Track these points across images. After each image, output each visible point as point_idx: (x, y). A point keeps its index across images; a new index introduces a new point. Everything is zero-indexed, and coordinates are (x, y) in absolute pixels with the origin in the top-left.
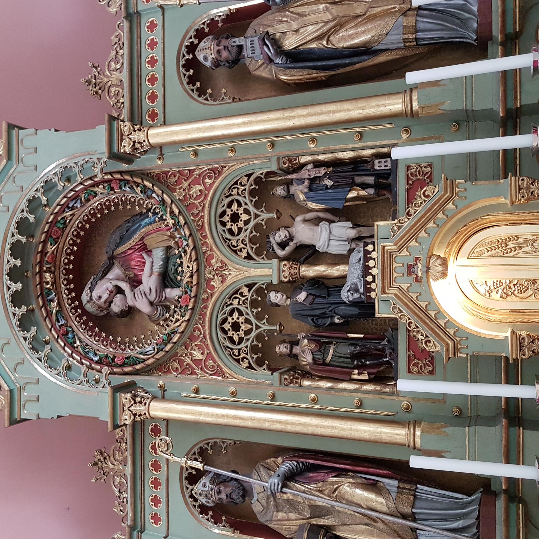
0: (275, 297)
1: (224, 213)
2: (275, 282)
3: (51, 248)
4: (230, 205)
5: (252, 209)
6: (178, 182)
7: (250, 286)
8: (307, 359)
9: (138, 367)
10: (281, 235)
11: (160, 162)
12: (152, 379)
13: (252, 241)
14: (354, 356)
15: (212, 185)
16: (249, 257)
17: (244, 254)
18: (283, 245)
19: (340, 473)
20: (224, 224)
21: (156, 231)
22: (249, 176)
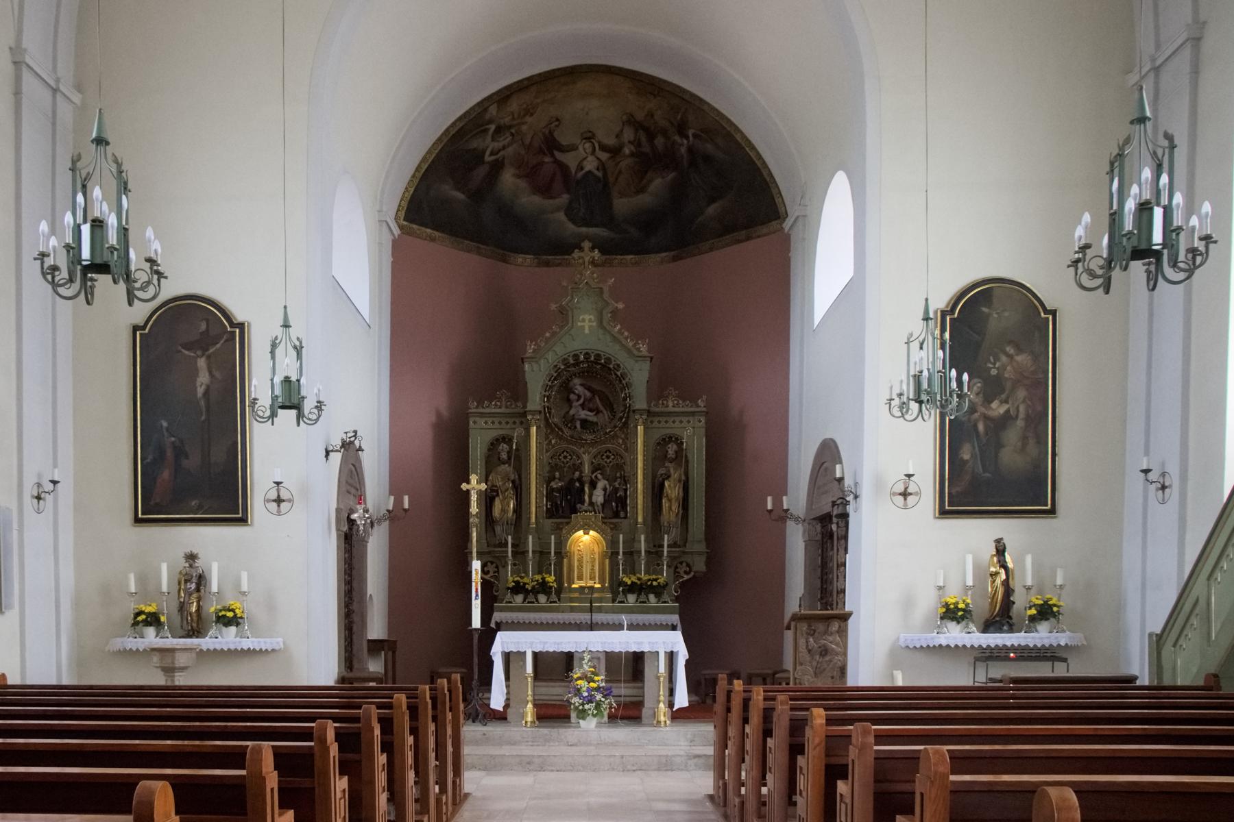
0: (577, 474)
1: (610, 452)
2: (583, 475)
3: (599, 367)
4: (613, 455)
5: (611, 464)
6: (623, 432)
7: (581, 463)
8: (554, 485)
9: (548, 415)
10: (599, 477)
11: (632, 425)
12: (543, 422)
13: (599, 464)
14: (557, 504)
15: (622, 448)
16: (592, 463)
17: (594, 461)
18: (596, 477)
19: (517, 500)
20: (606, 452)
21: (605, 419)
22: (624, 463)
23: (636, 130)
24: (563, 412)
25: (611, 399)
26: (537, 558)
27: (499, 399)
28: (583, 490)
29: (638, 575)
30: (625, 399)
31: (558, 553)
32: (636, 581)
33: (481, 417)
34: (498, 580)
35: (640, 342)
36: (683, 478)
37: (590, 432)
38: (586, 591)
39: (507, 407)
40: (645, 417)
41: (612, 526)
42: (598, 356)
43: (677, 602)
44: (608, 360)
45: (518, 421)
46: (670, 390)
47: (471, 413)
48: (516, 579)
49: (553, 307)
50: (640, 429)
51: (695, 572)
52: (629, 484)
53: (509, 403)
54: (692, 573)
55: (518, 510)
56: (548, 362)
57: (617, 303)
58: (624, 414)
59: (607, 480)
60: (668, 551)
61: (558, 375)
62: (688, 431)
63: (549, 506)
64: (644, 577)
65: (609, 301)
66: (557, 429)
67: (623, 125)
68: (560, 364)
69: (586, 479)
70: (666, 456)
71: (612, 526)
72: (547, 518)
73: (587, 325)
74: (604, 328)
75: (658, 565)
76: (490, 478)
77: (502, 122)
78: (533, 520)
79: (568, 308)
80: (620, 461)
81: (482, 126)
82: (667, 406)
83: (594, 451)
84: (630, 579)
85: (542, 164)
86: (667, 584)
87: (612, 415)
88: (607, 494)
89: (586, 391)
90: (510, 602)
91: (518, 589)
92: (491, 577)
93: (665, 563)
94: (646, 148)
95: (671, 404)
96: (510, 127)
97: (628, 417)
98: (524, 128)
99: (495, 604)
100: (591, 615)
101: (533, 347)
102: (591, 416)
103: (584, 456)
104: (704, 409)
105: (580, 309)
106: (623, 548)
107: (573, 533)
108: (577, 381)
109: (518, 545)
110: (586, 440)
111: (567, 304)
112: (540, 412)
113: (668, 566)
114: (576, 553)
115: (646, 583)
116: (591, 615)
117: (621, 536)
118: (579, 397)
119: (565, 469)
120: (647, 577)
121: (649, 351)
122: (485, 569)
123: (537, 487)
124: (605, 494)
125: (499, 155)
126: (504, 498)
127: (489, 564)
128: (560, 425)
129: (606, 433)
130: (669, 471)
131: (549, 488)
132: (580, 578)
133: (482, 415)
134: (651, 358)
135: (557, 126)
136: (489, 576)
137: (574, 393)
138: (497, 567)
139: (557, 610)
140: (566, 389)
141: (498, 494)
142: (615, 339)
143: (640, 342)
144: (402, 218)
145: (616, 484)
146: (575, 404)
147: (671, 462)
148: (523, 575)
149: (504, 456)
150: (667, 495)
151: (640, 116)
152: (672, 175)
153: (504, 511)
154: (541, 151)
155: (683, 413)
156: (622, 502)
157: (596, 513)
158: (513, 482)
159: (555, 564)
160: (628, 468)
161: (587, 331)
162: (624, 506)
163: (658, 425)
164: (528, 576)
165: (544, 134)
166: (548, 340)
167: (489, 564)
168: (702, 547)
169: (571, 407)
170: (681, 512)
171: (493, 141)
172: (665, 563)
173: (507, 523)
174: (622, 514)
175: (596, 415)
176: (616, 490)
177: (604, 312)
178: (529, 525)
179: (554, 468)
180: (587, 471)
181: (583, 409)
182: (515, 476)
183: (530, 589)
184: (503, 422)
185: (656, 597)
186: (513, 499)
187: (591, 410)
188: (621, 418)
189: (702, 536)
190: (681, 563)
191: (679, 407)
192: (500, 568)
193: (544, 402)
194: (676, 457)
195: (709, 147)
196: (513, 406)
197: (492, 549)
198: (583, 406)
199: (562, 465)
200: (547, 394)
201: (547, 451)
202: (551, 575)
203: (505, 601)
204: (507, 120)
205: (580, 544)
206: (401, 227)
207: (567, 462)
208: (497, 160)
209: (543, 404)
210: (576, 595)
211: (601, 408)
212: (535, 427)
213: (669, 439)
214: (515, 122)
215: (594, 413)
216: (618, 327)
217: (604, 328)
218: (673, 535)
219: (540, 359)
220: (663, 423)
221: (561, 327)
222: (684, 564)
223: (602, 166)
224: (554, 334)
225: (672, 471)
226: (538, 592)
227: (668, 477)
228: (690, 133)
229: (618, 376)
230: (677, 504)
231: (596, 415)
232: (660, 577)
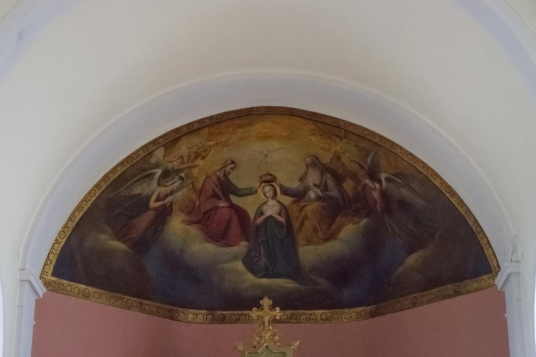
23: (322, 173)
67: (307, 168)
77: (170, 166)
81: (146, 170)
85: (216, 208)
94: (334, 192)
96: (178, 171)
98: (195, 171)
125: (166, 201)
144: (50, 274)
151: (326, 158)
154: (215, 196)
165: (219, 179)
204: (176, 164)
206: (47, 284)
208: (164, 205)
223: (284, 210)
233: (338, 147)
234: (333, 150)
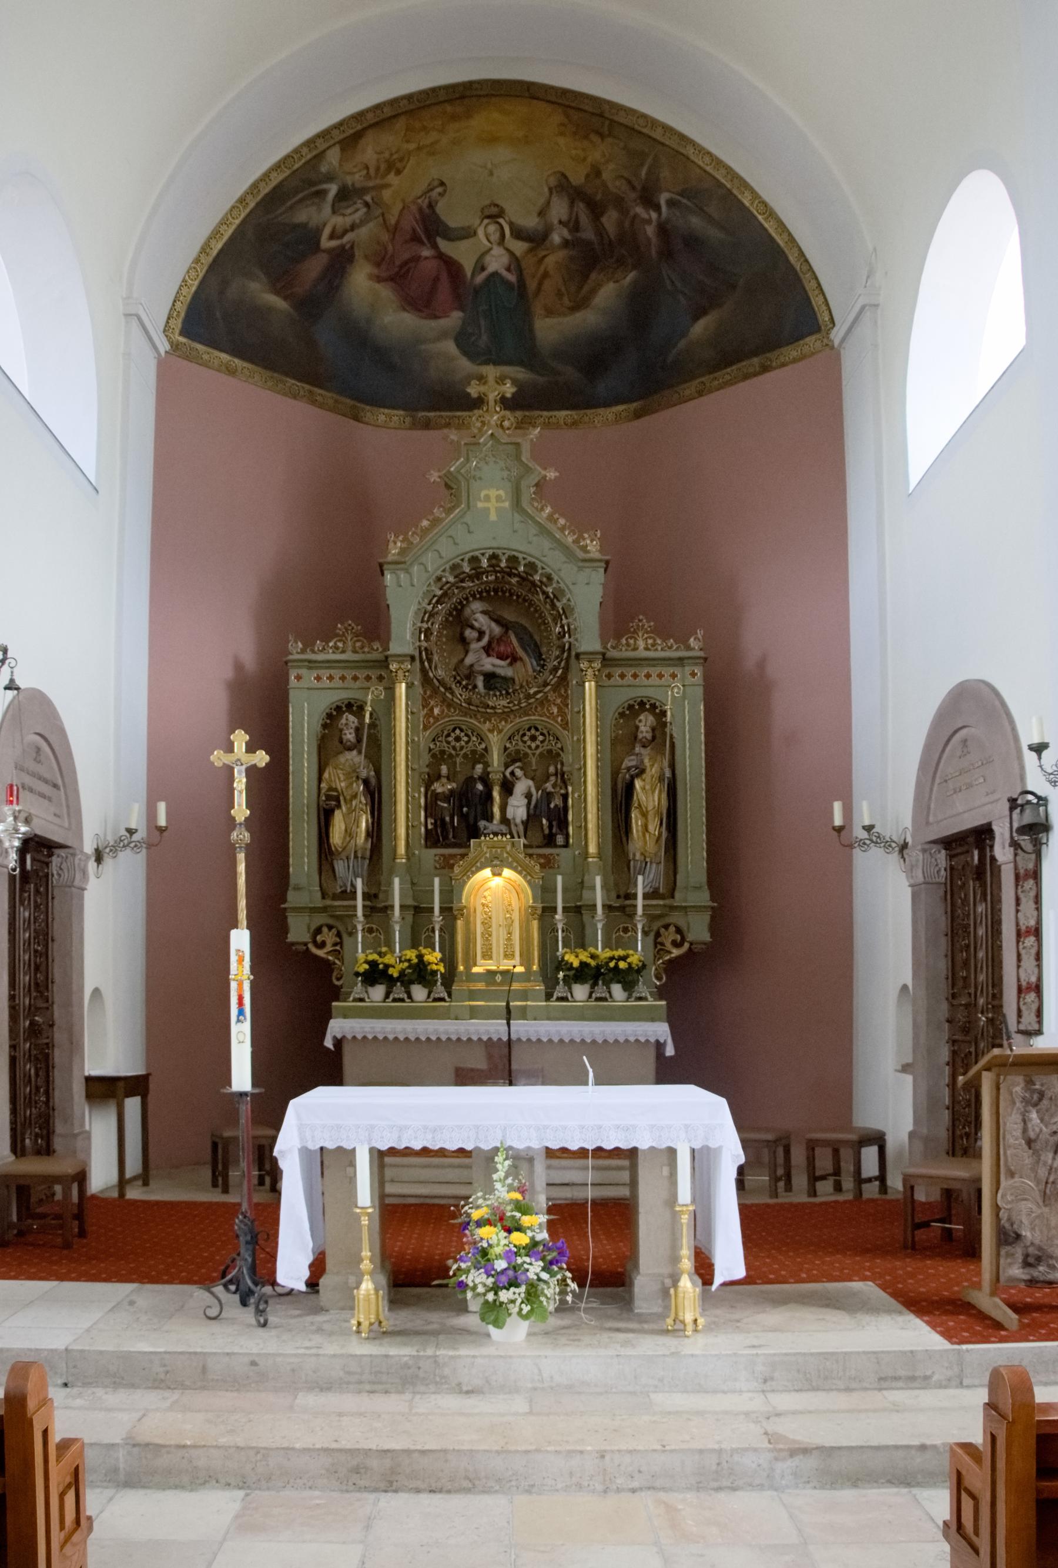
0: (479, 768)
1: (537, 729)
2: (489, 769)
3: (514, 580)
4: (542, 734)
5: (538, 752)
6: (561, 696)
7: (486, 749)
9: (426, 664)
10: (519, 773)
12: (418, 675)
14: (443, 820)
15: (557, 722)
16: (506, 749)
17: (508, 745)
18: (512, 773)
20: (529, 729)
22: (562, 749)
24: (454, 661)
25: (537, 638)
26: (409, 918)
27: (342, 638)
28: (489, 797)
29: (592, 950)
30: (562, 636)
31: (447, 910)
32: (589, 961)
33: (310, 668)
34: (342, 960)
35: (586, 535)
36: (668, 773)
37: (501, 695)
38: (499, 978)
39: (355, 652)
40: (597, 665)
41: (542, 861)
42: (513, 560)
43: (661, 999)
44: (532, 567)
45: (374, 674)
46: (640, 621)
47: (291, 661)
48: (371, 958)
49: (434, 476)
50: (590, 687)
51: (691, 944)
52: (572, 785)
53: (358, 644)
54: (686, 945)
55: (376, 833)
56: (427, 571)
57: (545, 469)
58: (559, 663)
59: (533, 779)
60: (644, 906)
61: (445, 594)
62: (676, 690)
63: (430, 827)
64: (604, 954)
65: (530, 465)
66: (442, 689)
67: (551, 193)
68: (447, 574)
69: (495, 777)
70: (636, 737)
71: (542, 861)
72: (426, 847)
73: (492, 505)
74: (523, 512)
75: (626, 930)
76: (326, 775)
77: (349, 180)
78: (402, 849)
79: (460, 478)
80: (556, 747)
81: (312, 183)
82: (635, 649)
83: (508, 727)
84: (577, 956)
86: (644, 966)
87: (538, 665)
88: (532, 806)
89: (493, 625)
90: (361, 1000)
91: (375, 975)
92: (328, 953)
93: (640, 927)
95: (641, 644)
97: (567, 669)
98: (386, 194)
99: (334, 1004)
100: (509, 1024)
101: (399, 544)
102: (502, 668)
103: (490, 735)
104: (701, 654)
105: (480, 478)
106: (564, 901)
107: (474, 873)
108: (477, 606)
109: (376, 896)
110: (493, 708)
111: (459, 472)
112: (413, 658)
113: (645, 933)
114: (479, 909)
115: (607, 963)
116: (509, 1024)
117: (559, 878)
118: (481, 634)
119: (458, 760)
120: (608, 953)
121: (601, 551)
122: (319, 938)
123: (407, 792)
124: (529, 803)
126: (351, 811)
127: (325, 930)
128: (449, 681)
129: (528, 697)
130: (642, 762)
131: (429, 793)
132: (487, 955)
133: (311, 664)
134: (607, 563)
135: (441, 195)
136: (325, 950)
137: (472, 627)
138: (339, 935)
139: (444, 1015)
140: (458, 620)
141: (339, 802)
142: (543, 531)
143: (586, 535)
144: (177, 331)
145: (549, 786)
146: (474, 646)
147: (644, 746)
148: (384, 949)
149: (350, 736)
150: (639, 805)
152: (631, 276)
153: (349, 833)
154: (415, 239)
155: (664, 659)
156: (560, 819)
157: (512, 837)
158: (366, 782)
159: (441, 930)
160: (568, 758)
161: (493, 517)
162: (563, 824)
163: (620, 682)
164: (393, 952)
166: (426, 531)
167: (325, 930)
168: (703, 898)
169: (467, 652)
170: (664, 835)
171: (334, 212)
172: (640, 927)
173: (356, 857)
174: (560, 840)
175: (511, 664)
176: (549, 796)
177: (524, 484)
178: (395, 859)
179: (438, 757)
180: (496, 764)
181: (489, 655)
182: (368, 772)
183: (396, 975)
184: (349, 677)
185: (625, 989)
186: (366, 813)
187: (501, 657)
188: (555, 669)
189: (703, 878)
190: (666, 927)
191: (656, 650)
192: (345, 936)
193: (420, 640)
194: (654, 738)
195: (695, 222)
196: (366, 650)
197: (328, 902)
198: (488, 650)
199: (453, 752)
200: (425, 625)
201: (425, 728)
202: (434, 950)
203: (351, 999)
204: (357, 179)
205: (486, 894)
207: (462, 748)
208: (342, 247)
209: (418, 644)
210: (481, 986)
211: (520, 652)
212: (404, 685)
213: (641, 706)
214: (371, 184)
215: (508, 661)
216: (548, 510)
217: (523, 512)
218: (651, 876)
219: (411, 564)
220: (629, 679)
221: (449, 511)
222: (672, 929)
224: (436, 522)
225: (647, 762)
226: (412, 982)
227: (641, 772)
228: (663, 198)
229: (548, 597)
230: (657, 821)
231: (511, 664)
232: (631, 952)
233: (598, 152)
234: (589, 159)
